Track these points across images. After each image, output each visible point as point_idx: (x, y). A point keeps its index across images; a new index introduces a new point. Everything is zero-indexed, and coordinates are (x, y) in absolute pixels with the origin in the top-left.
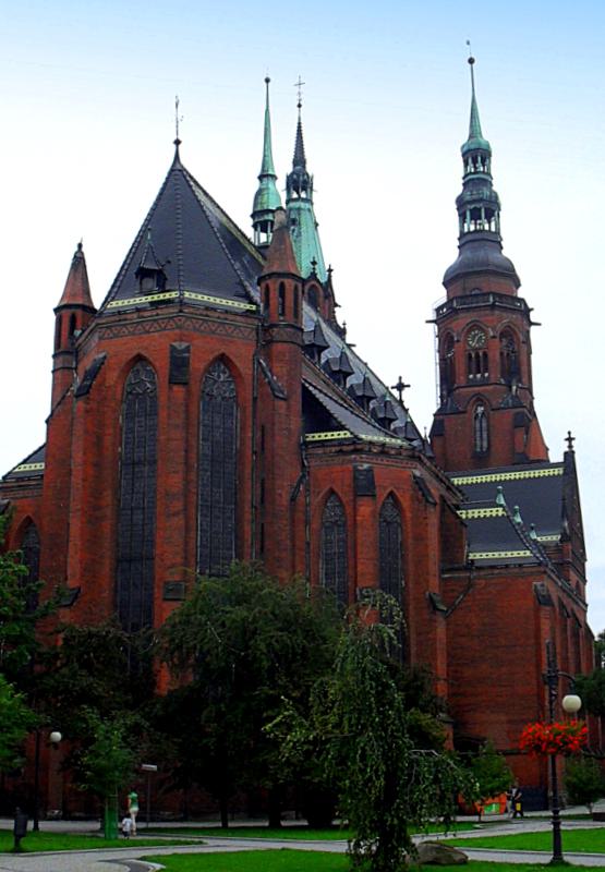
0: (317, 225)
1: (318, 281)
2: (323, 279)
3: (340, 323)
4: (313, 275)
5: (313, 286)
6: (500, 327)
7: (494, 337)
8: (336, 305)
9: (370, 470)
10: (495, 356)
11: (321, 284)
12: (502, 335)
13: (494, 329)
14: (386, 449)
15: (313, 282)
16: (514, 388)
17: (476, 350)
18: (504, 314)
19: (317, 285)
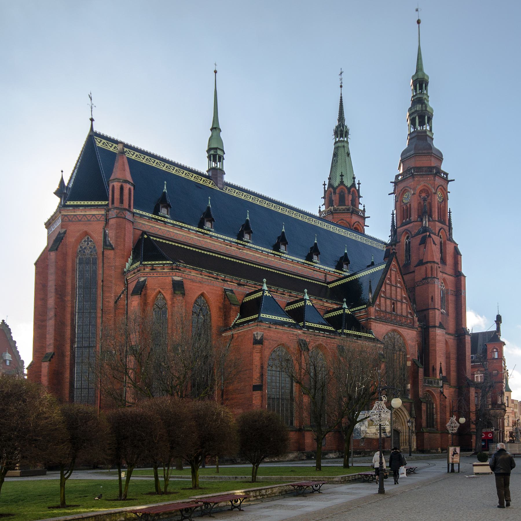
0: (348, 154)
1: (344, 185)
2: (348, 184)
3: (361, 207)
4: (342, 183)
5: (342, 188)
6: (419, 188)
7: (414, 194)
8: (360, 197)
9: (145, 281)
10: (415, 205)
11: (346, 187)
12: (421, 191)
13: (414, 189)
14: (154, 268)
15: (342, 187)
16: (424, 222)
17: (406, 204)
18: (422, 179)
19: (345, 188)
